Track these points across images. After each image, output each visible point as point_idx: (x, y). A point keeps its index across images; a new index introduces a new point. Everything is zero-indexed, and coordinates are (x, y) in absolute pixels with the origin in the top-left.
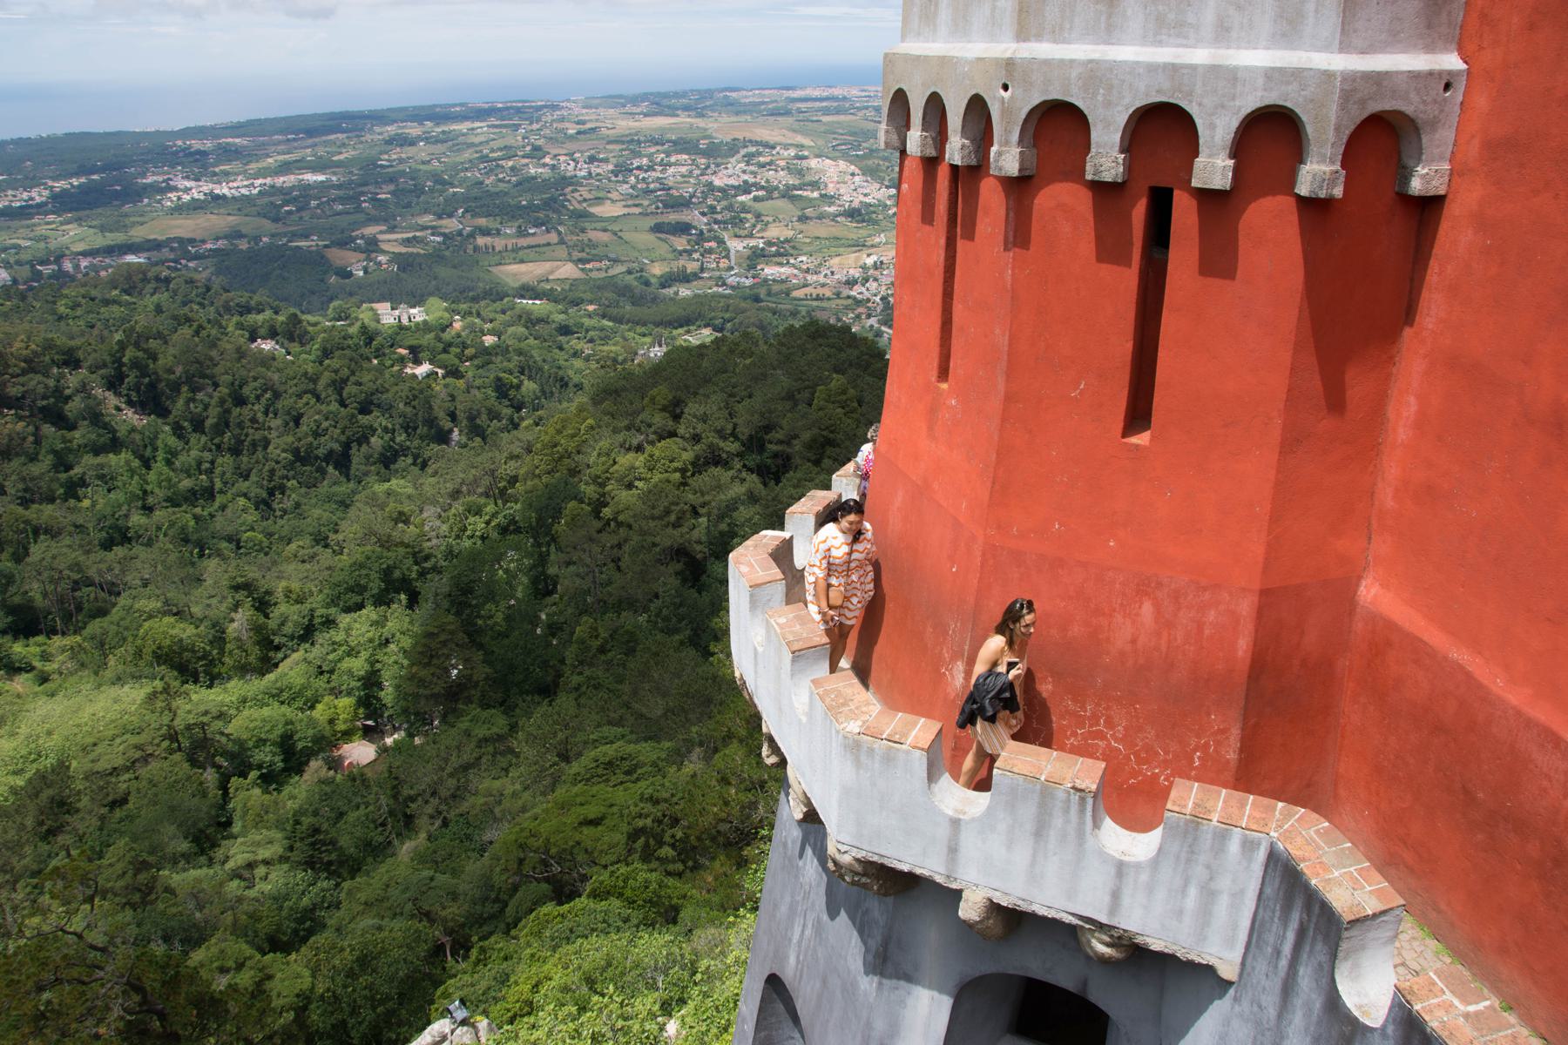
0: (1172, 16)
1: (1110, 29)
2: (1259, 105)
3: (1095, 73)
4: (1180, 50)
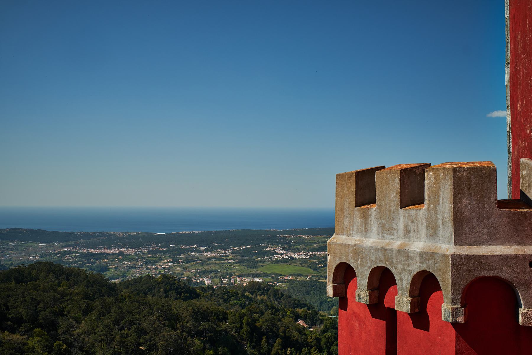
0: (387, 225)
1: (366, 230)
2: (418, 270)
3: (357, 251)
4: (391, 241)
